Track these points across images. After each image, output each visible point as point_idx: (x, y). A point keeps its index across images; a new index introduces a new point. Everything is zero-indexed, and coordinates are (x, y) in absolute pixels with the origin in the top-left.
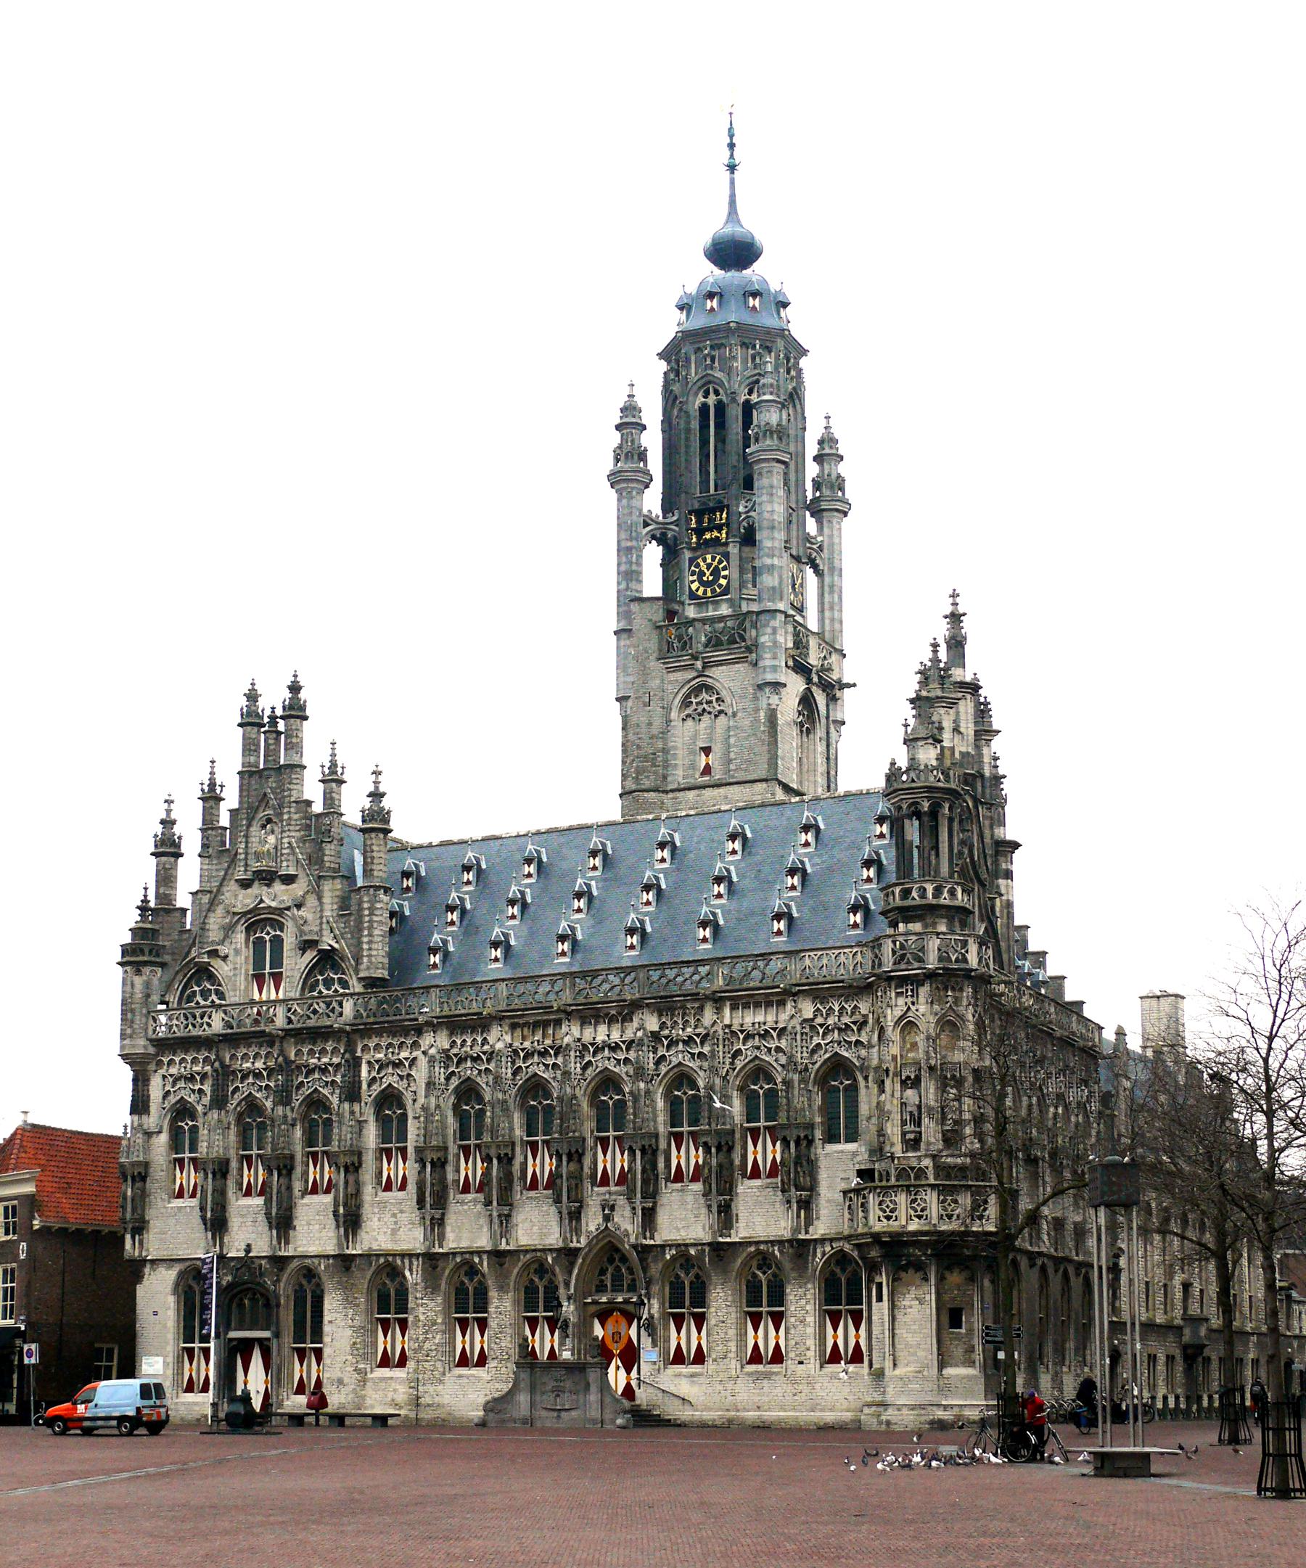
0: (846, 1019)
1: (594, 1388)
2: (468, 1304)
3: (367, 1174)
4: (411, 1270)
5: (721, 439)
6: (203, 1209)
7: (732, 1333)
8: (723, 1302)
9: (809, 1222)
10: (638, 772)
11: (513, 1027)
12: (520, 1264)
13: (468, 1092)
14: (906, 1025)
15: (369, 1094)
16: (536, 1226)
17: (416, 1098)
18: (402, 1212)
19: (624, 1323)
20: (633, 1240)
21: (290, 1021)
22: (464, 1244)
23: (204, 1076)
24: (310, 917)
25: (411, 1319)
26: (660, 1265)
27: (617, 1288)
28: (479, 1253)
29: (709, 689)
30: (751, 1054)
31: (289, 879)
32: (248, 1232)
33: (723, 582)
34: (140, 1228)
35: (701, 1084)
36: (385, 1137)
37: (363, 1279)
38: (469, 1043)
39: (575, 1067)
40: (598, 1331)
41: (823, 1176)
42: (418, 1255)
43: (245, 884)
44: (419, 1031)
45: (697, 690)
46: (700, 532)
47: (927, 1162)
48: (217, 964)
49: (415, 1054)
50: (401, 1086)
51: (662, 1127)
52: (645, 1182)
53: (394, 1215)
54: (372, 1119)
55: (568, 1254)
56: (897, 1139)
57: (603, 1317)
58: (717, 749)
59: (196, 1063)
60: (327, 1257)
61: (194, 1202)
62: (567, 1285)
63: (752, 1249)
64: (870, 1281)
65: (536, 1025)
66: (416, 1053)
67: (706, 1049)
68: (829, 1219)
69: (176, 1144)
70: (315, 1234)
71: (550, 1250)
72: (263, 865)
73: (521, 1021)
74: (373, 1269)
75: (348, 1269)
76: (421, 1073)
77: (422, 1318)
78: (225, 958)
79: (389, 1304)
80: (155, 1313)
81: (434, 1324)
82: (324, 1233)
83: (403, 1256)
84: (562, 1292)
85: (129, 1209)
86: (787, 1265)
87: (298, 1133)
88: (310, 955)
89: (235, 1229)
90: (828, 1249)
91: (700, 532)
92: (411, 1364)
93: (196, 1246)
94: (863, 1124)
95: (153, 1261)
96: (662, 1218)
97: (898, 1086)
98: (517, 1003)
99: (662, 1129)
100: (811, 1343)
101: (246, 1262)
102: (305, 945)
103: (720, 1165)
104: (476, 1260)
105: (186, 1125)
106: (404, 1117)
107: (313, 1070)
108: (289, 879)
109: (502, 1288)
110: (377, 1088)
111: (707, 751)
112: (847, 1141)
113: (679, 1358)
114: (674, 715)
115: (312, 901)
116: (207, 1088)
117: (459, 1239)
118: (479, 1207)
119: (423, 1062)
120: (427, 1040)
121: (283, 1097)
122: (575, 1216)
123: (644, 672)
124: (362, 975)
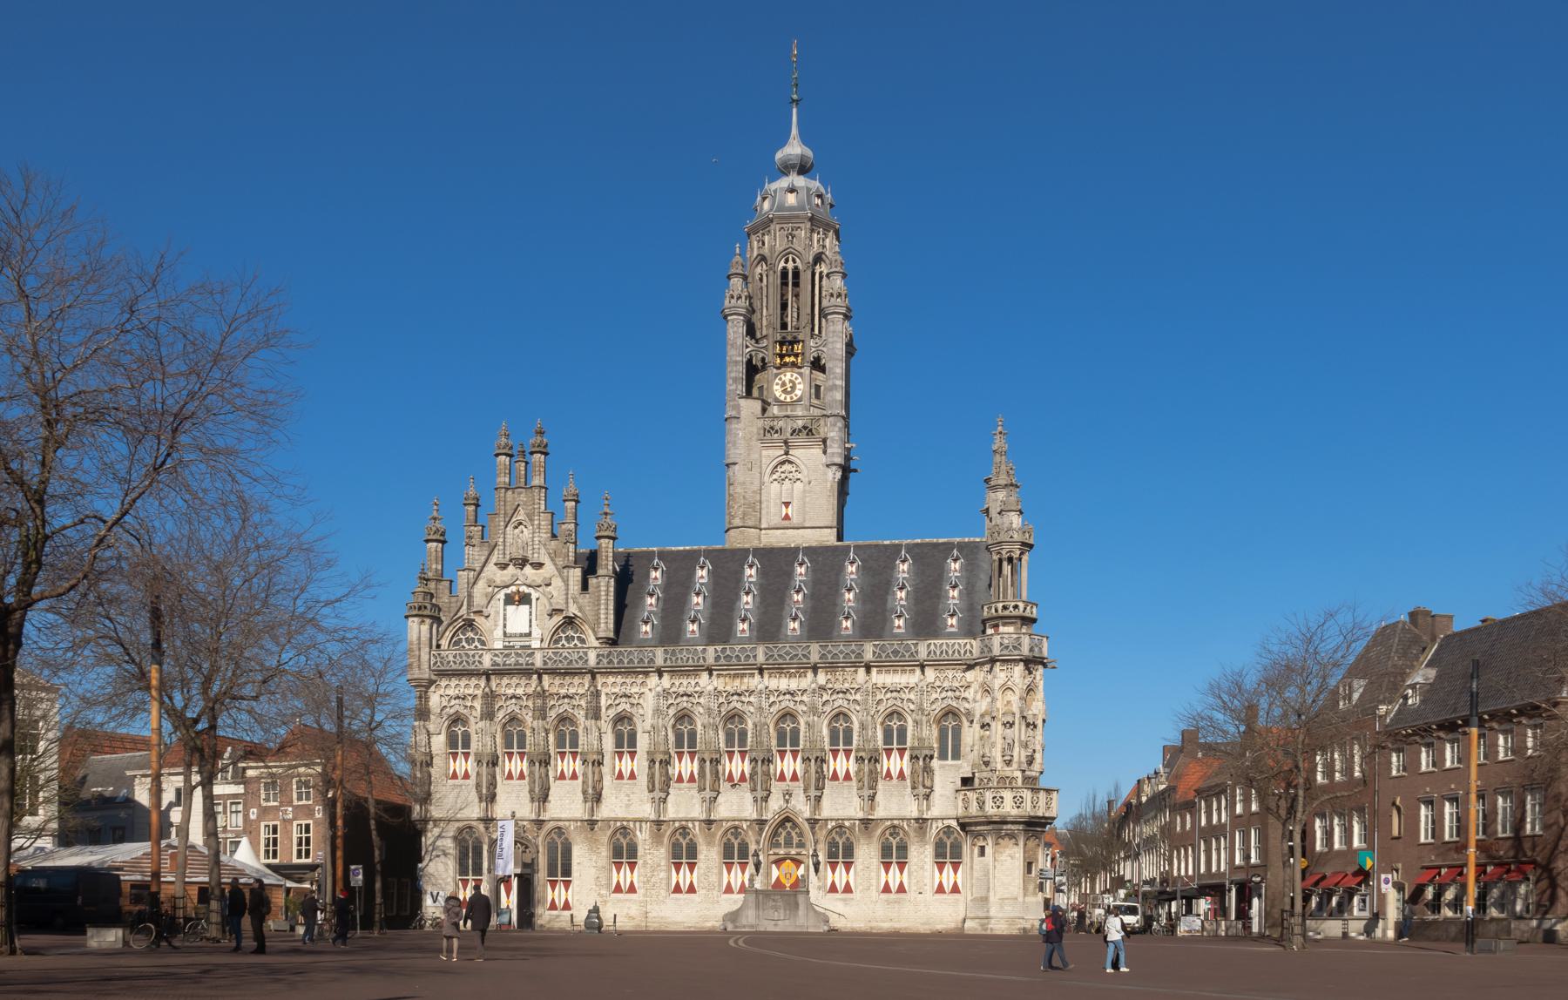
0: (956, 684)
1: (802, 907)
2: (684, 853)
3: (606, 769)
5: (797, 296)
6: (478, 786)
7: (873, 874)
8: (867, 854)
9: (928, 808)
10: (744, 514)
13: (684, 717)
14: (1006, 688)
15: (607, 715)
16: (736, 805)
17: (645, 722)
19: (792, 865)
20: (807, 815)
21: (545, 663)
22: (681, 815)
23: (475, 697)
24: (555, 594)
25: (640, 862)
26: (824, 832)
27: (788, 843)
28: (693, 821)
30: (890, 703)
31: (539, 565)
33: (799, 393)
34: (426, 799)
35: (854, 718)
36: (619, 743)
38: (685, 684)
39: (765, 705)
40: (775, 873)
41: (937, 779)
43: (504, 566)
44: (646, 674)
45: (783, 463)
46: (782, 356)
47: (1019, 774)
48: (479, 620)
50: (634, 711)
51: (827, 747)
52: (818, 780)
54: (610, 731)
55: (761, 823)
56: (999, 759)
57: (778, 862)
58: (795, 503)
59: (475, 687)
61: (472, 781)
62: (758, 843)
65: (736, 676)
66: (645, 690)
67: (858, 697)
68: (945, 804)
69: (452, 741)
70: (566, 804)
72: (519, 554)
76: (649, 702)
79: (624, 852)
83: (635, 821)
84: (752, 848)
86: (912, 834)
87: (551, 738)
91: (782, 356)
92: (640, 892)
94: (965, 749)
96: (825, 802)
97: (1000, 727)
98: (722, 661)
99: (827, 747)
100: (928, 881)
102: (555, 611)
103: (871, 772)
105: (459, 729)
108: (539, 565)
109: (709, 844)
110: (612, 713)
111: (787, 504)
112: (954, 758)
113: (833, 889)
114: (766, 478)
115: (557, 582)
116: (477, 704)
117: (677, 812)
118: (694, 792)
121: (542, 713)
122: (766, 799)
123: (749, 449)
124: (601, 635)
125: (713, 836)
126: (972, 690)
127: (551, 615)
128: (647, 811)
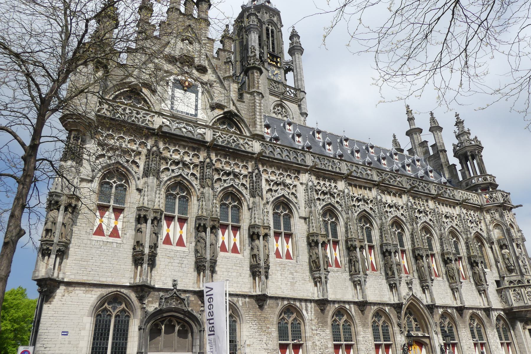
4: (306, 310)
11: (350, 185)
12: (372, 311)
18: (296, 272)
22: (339, 297)
25: (309, 344)
28: (349, 303)
29: (282, 107)
31: (202, 70)
32: (173, 269)
37: (272, 313)
42: (311, 301)
49: (295, 183)
50: (292, 198)
53: (292, 273)
55: (398, 307)
60: (244, 296)
63: (471, 311)
64: (524, 329)
65: (360, 187)
66: (296, 183)
71: (388, 305)
73: (353, 183)
74: (280, 307)
75: (261, 307)
77: (318, 343)
78: (154, 92)
80: (65, 333)
81: (327, 348)
82: (240, 279)
83: (301, 300)
85: (57, 234)
88: (218, 112)
89: (162, 267)
90: (496, 313)
93: (123, 273)
95: (69, 284)
101: (174, 294)
104: (347, 306)
106: (288, 217)
107: (228, 174)
108: (202, 70)
109: (364, 325)
118: (347, 275)
119: (301, 189)
120: (304, 177)
125: (366, 319)
126: (483, 224)
127: (213, 108)
128: (309, 290)
